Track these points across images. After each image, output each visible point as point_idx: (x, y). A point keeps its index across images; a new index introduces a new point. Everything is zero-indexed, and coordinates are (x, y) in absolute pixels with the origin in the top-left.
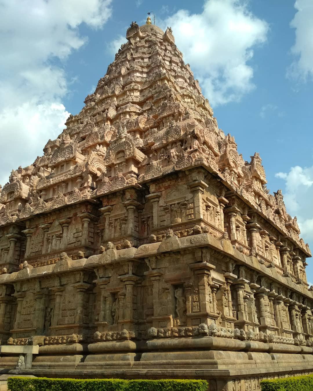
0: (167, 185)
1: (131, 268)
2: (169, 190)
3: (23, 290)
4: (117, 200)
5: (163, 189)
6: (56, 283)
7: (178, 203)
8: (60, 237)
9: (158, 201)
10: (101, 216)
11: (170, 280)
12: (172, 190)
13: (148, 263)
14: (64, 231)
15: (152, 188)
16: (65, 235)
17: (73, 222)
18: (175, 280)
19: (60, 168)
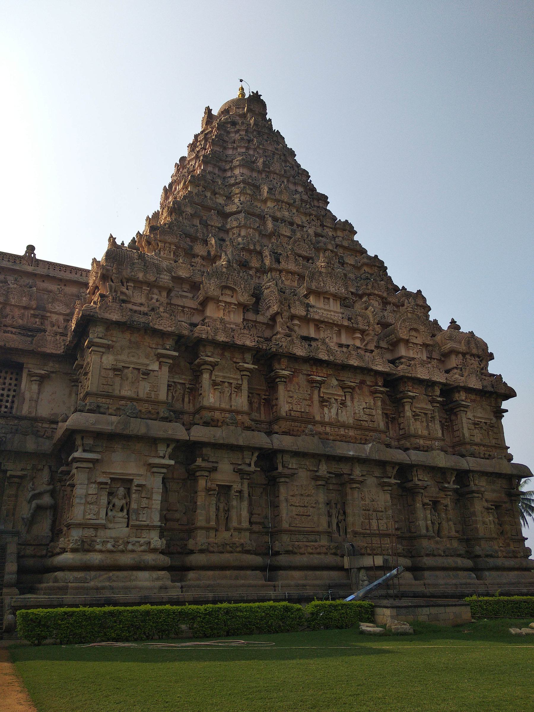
0: (472, 398)
6: (357, 472)
8: (343, 404)
16: (349, 403)
17: (357, 389)
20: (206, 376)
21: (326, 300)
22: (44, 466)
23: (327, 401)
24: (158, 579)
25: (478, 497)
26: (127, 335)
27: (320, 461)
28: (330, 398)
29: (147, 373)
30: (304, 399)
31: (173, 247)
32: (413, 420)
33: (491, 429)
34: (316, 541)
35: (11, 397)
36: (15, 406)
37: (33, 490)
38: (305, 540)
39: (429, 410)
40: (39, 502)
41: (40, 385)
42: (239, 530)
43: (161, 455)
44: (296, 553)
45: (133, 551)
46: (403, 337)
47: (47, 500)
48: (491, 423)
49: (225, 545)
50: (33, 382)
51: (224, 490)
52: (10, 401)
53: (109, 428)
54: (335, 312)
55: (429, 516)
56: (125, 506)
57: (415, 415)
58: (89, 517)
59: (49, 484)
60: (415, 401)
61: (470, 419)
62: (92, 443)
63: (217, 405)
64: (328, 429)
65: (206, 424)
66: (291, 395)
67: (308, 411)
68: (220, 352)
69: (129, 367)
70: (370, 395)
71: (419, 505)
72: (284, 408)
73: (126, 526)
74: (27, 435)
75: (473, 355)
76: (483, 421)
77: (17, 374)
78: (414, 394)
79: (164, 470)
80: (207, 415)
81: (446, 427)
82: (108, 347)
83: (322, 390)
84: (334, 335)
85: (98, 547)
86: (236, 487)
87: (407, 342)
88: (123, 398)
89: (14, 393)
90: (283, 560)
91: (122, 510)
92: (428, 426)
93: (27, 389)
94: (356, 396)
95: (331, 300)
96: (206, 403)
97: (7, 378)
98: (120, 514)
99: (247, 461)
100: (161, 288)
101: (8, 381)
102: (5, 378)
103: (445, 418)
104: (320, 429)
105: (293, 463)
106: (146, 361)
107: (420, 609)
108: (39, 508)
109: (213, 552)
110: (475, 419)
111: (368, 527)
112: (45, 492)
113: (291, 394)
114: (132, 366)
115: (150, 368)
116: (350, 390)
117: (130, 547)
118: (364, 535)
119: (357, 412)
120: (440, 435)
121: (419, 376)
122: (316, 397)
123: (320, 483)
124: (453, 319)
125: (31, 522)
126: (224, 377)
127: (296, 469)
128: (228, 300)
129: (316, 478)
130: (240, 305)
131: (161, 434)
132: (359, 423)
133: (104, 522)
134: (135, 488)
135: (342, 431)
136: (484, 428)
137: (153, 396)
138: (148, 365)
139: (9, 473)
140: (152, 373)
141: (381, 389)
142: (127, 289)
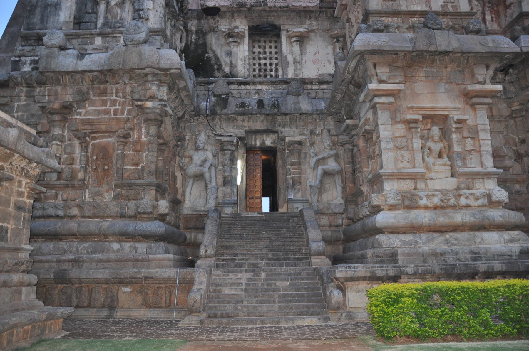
22: (322, 130)
24: (512, 241)
35: (274, 65)
36: (280, 73)
37: (316, 155)
40: (325, 167)
41: (301, 46)
43: (481, 79)
45: (468, 206)
47: (332, 165)
50: (293, 44)
52: (274, 69)
56: (443, 149)
58: (401, 165)
59: (331, 149)
62: (388, 70)
73: (450, 174)
74: (299, 95)
77: (276, 42)
79: (488, 100)
85: (423, 202)
89: (276, 61)
91: (440, 156)
93: (288, 52)
97: (267, 47)
98: (440, 161)
101: (268, 50)
102: (265, 48)
108: (326, 174)
112: (329, 157)
117: (463, 201)
125: (321, 189)
133: (423, 170)
134: (454, 125)
139: (287, 139)
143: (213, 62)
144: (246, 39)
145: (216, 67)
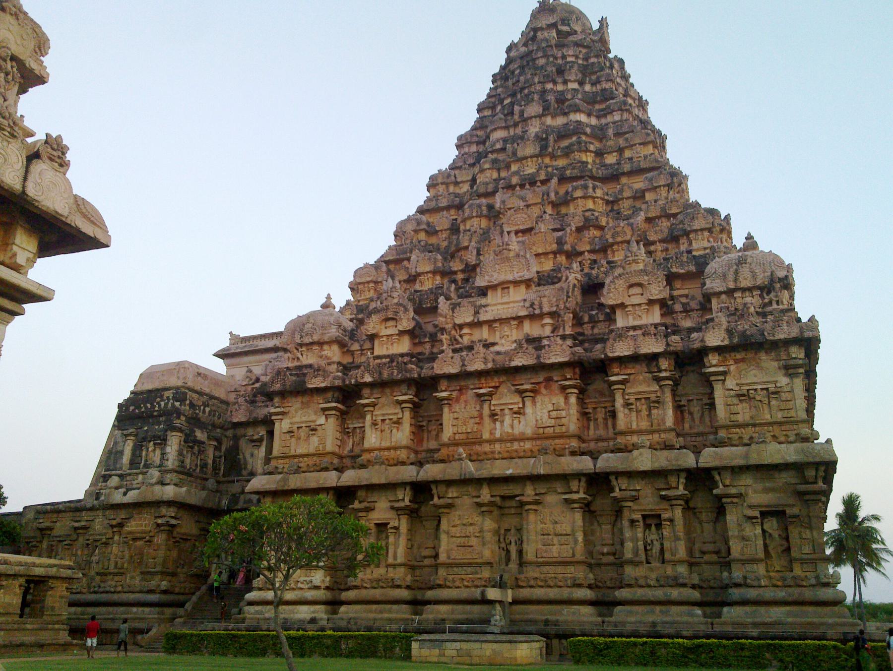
1: (682, 480)
2: (742, 366)
3: (450, 495)
4: (638, 366)
5: (732, 362)
6: (529, 492)
7: (762, 389)
8: (520, 412)
9: (724, 381)
10: (589, 384)
11: (759, 506)
12: (750, 367)
13: (717, 477)
14: (528, 403)
15: (713, 359)
16: (529, 410)
17: (543, 391)
18: (766, 506)
19: (499, 290)
20: (368, 417)
21: (506, 290)
23: (497, 415)
24: (314, 612)
25: (732, 503)
26: (300, 399)
27: (481, 485)
28: (504, 409)
29: (315, 430)
30: (472, 418)
31: (372, 285)
32: (626, 411)
33: (773, 396)
34: (476, 573)
38: (463, 572)
39: (650, 392)
42: (394, 566)
44: (449, 587)
45: (302, 589)
46: (611, 303)
48: (776, 387)
49: (378, 580)
51: (382, 527)
53: (272, 487)
54: (514, 302)
55: (640, 535)
57: (627, 405)
60: (628, 385)
61: (732, 390)
63: (377, 445)
64: (497, 447)
65: (363, 466)
66: (456, 417)
67: (475, 430)
68: (380, 390)
69: (301, 427)
70: (562, 392)
71: (626, 523)
72: (447, 434)
75: (750, 289)
76: (759, 387)
78: (620, 378)
80: (365, 457)
81: (707, 407)
82: (283, 413)
83: (493, 402)
84: (514, 331)
86: (393, 524)
87: (622, 306)
88: (295, 456)
90: (430, 594)
92: (649, 415)
94: (539, 398)
95: (511, 289)
96: (367, 445)
99: (401, 498)
100: (330, 343)
103: (705, 394)
104: (487, 448)
105: (452, 492)
106: (313, 417)
107: (448, 644)
109: (366, 588)
110: (742, 388)
111: (544, 555)
113: (456, 415)
114: (304, 425)
115: (318, 423)
116: (531, 394)
117: (300, 585)
118: (538, 565)
119: (539, 418)
120: (670, 421)
121: (616, 354)
122: (486, 411)
123: (484, 509)
124: (749, 234)
126: (383, 415)
127: (456, 497)
128: (389, 332)
129: (479, 505)
130: (401, 333)
131: (313, 485)
132: (541, 431)
135: (516, 446)
136: (758, 398)
137: (321, 449)
138: (315, 421)
140: (319, 428)
141: (567, 383)
142: (302, 355)
143: (242, 462)
144: (264, 443)
145: (243, 466)
